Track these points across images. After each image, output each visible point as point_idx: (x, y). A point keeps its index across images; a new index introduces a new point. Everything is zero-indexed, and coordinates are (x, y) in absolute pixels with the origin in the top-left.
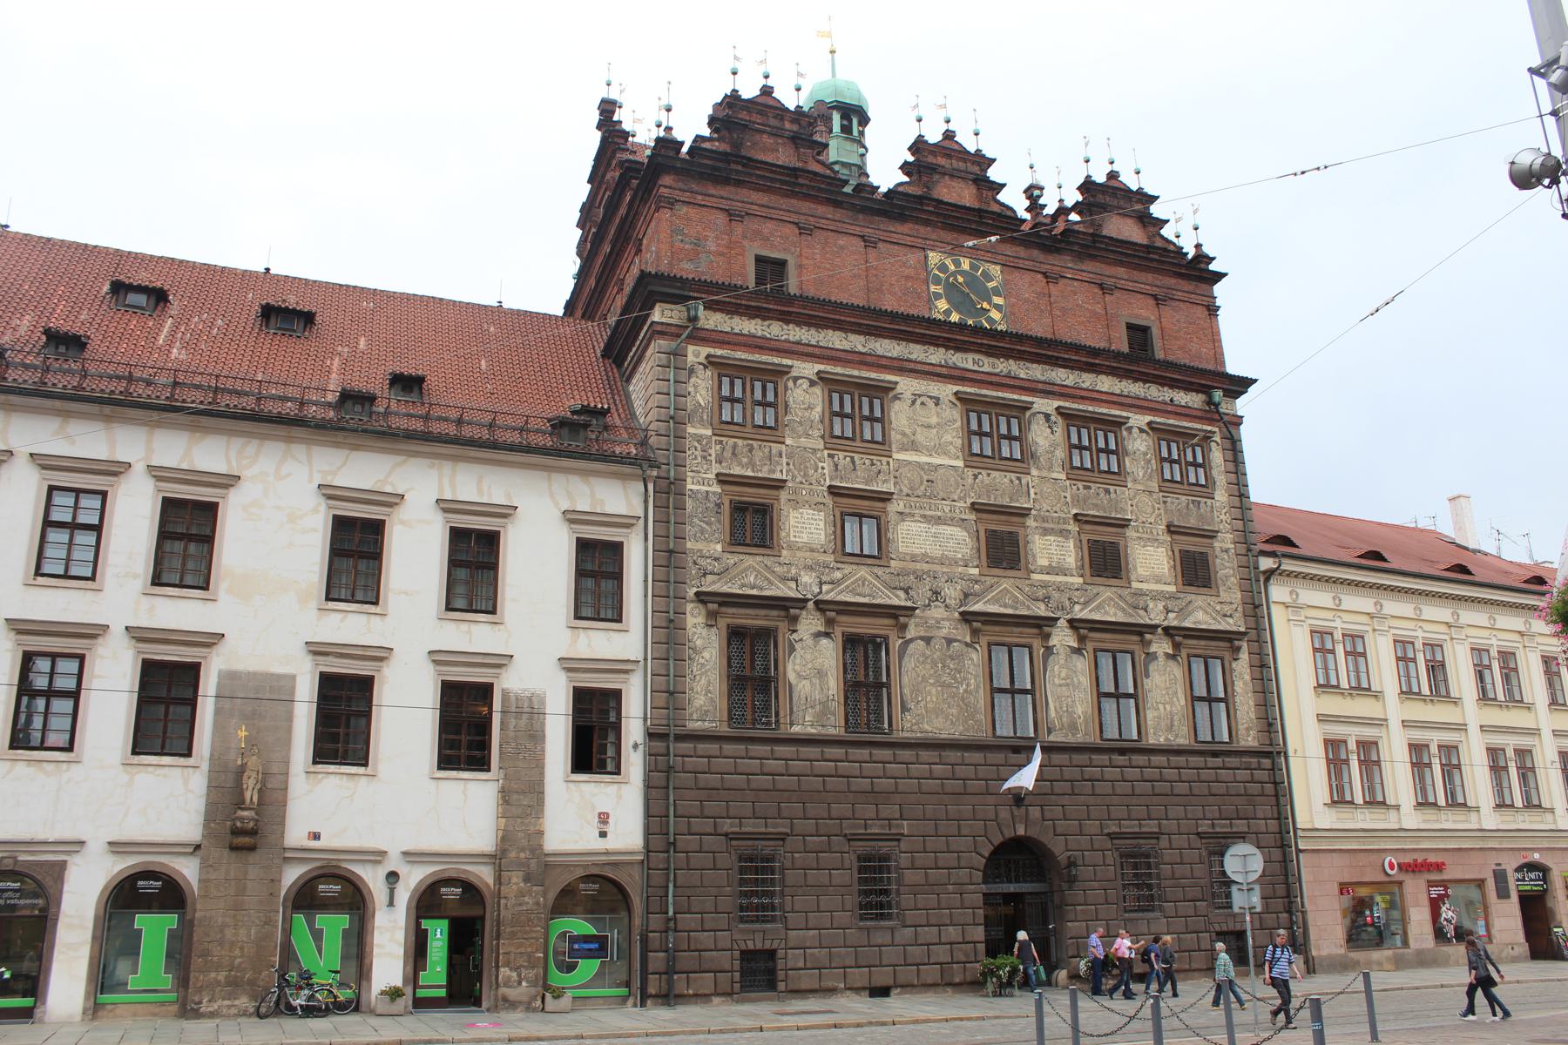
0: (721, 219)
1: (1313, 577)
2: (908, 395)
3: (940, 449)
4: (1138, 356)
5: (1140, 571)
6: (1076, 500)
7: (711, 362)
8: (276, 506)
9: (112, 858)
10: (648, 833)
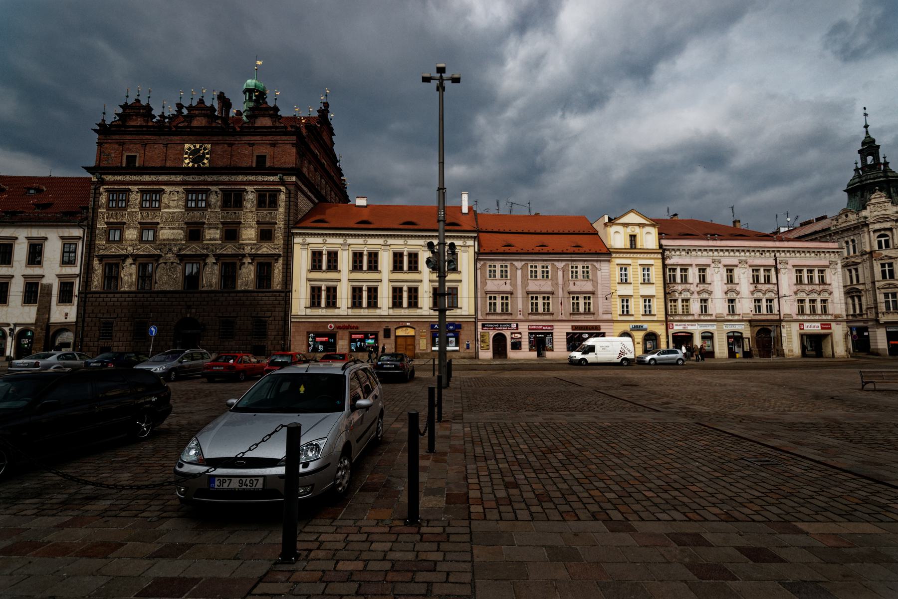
1: (311, 234)
3: (177, 207)
6: (223, 217)
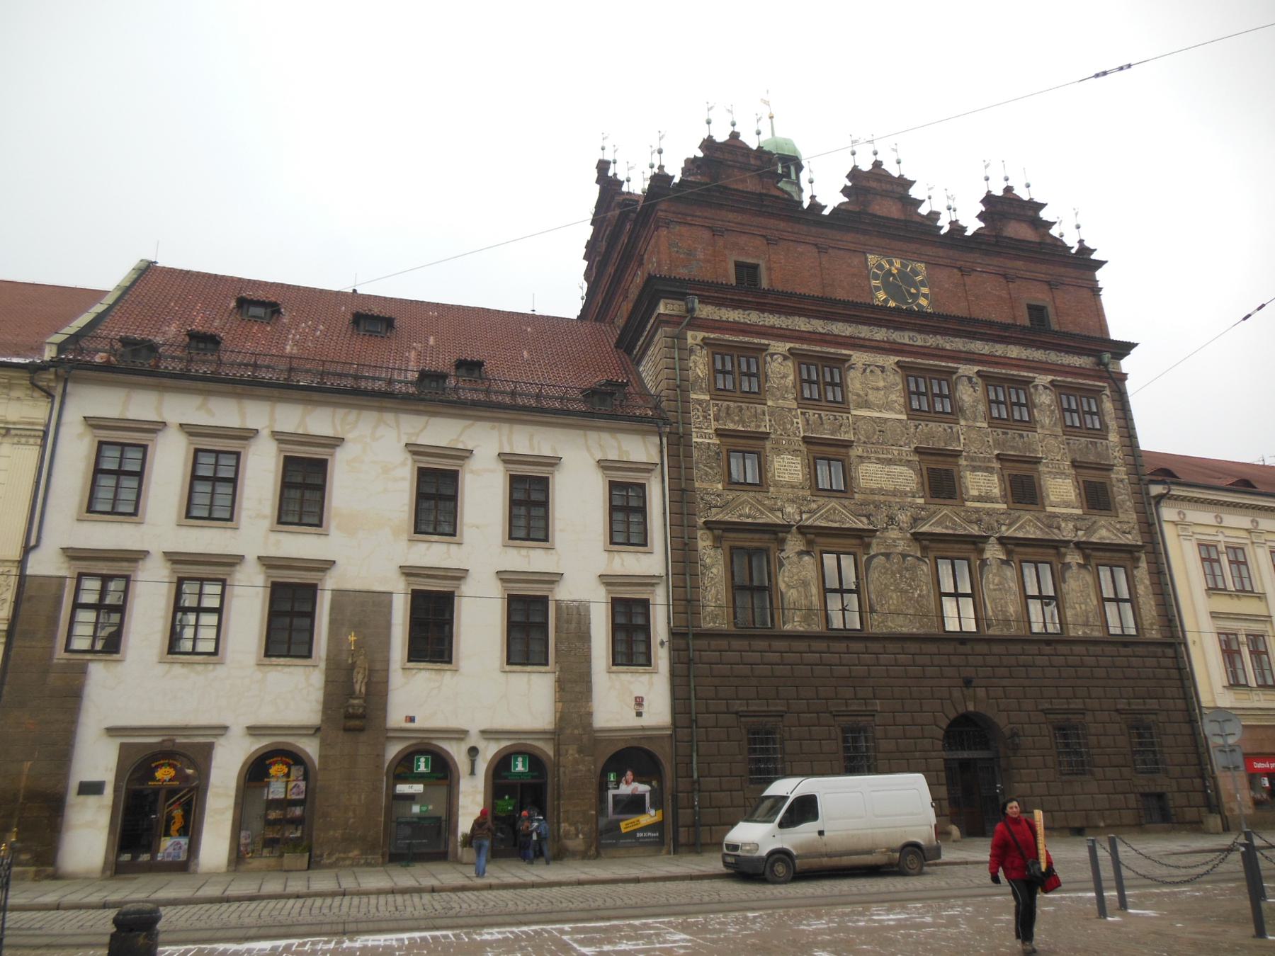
0: (706, 235)
2: (860, 365)
3: (888, 407)
4: (1037, 329)
5: (1052, 498)
6: (997, 444)
7: (706, 343)
8: (373, 462)
9: (249, 740)
10: (674, 712)
